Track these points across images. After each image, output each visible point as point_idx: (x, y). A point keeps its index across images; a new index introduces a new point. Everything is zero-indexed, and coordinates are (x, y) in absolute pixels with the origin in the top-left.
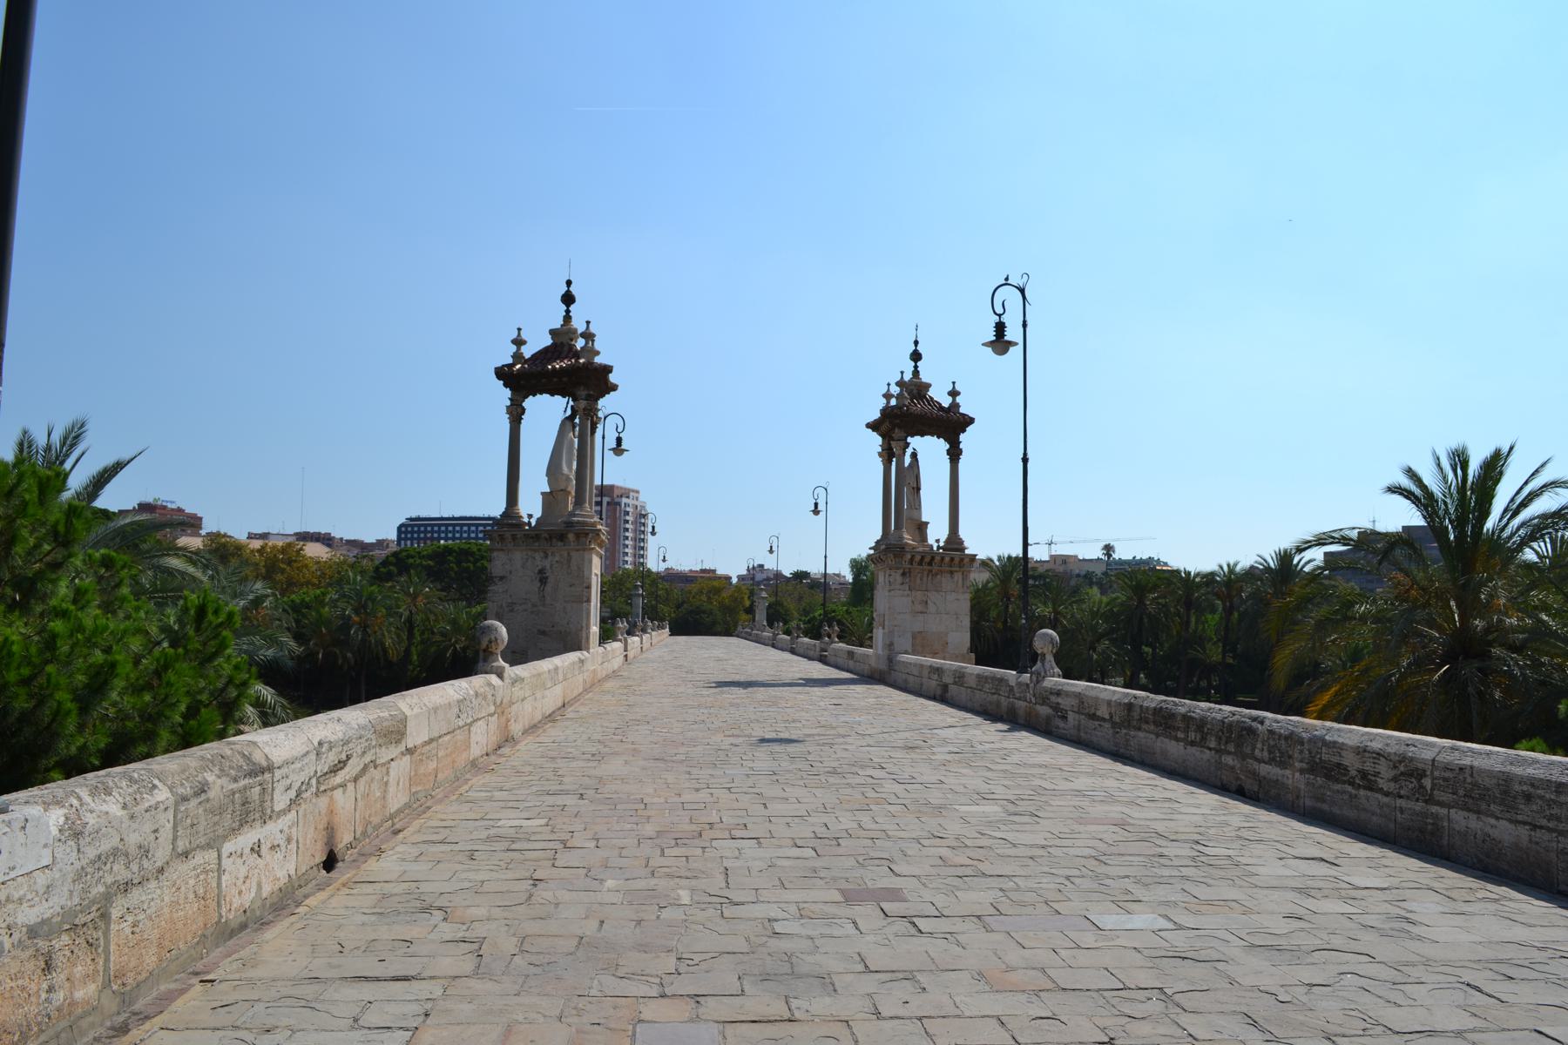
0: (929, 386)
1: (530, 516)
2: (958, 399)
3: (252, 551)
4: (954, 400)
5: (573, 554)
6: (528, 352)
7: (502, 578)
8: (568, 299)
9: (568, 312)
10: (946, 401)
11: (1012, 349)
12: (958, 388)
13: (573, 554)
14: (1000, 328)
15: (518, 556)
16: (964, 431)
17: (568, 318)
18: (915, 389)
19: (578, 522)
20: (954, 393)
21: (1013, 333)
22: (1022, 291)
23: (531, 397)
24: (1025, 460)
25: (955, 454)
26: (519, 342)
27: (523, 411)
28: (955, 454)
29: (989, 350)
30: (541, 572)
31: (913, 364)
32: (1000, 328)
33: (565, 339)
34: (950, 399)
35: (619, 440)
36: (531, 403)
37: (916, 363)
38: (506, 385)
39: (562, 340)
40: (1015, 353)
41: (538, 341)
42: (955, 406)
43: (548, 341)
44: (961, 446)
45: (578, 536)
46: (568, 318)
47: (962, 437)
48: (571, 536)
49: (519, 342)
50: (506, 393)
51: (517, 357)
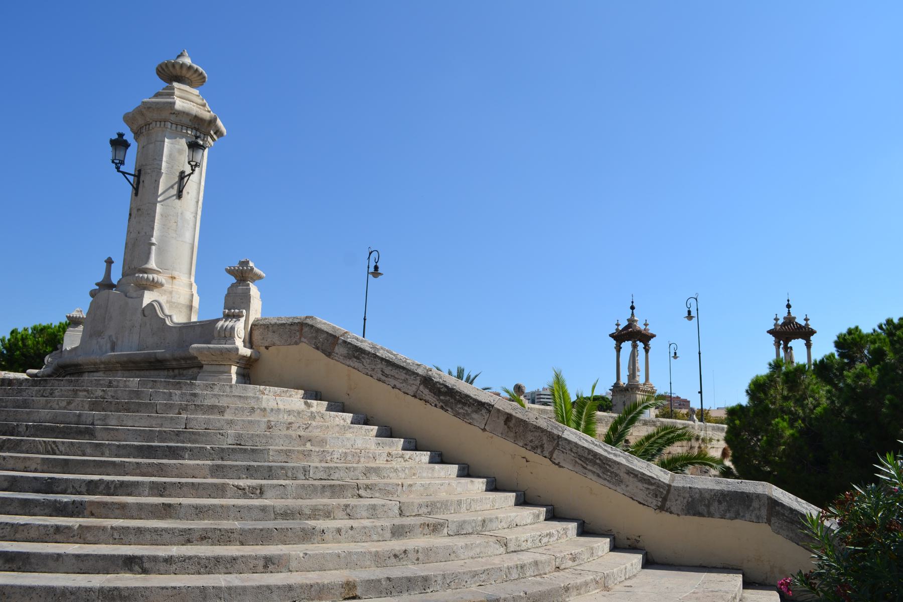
0: (795, 318)
1: (624, 384)
2: (809, 322)
3: (683, 414)
4: (807, 322)
5: (631, 395)
6: (620, 328)
7: (615, 405)
8: (632, 308)
9: (633, 312)
10: (803, 323)
11: (694, 319)
12: (808, 317)
13: (631, 395)
14: (689, 312)
15: (618, 397)
16: (812, 335)
17: (633, 314)
18: (789, 320)
19: (632, 385)
20: (806, 320)
21: (693, 314)
22: (696, 299)
23: (623, 343)
24: (700, 353)
25: (808, 345)
26: (618, 325)
27: (621, 348)
28: (808, 345)
29: (686, 319)
30: (624, 402)
31: (788, 309)
32: (689, 312)
33: (631, 322)
34: (805, 322)
35: (675, 353)
36: (624, 345)
37: (789, 309)
38: (614, 340)
39: (631, 322)
40: (695, 320)
41: (624, 324)
42: (807, 325)
43: (627, 323)
44: (811, 342)
45: (632, 389)
46: (633, 314)
47: (812, 338)
48: (629, 389)
49: (618, 325)
50: (613, 342)
51: (617, 330)
